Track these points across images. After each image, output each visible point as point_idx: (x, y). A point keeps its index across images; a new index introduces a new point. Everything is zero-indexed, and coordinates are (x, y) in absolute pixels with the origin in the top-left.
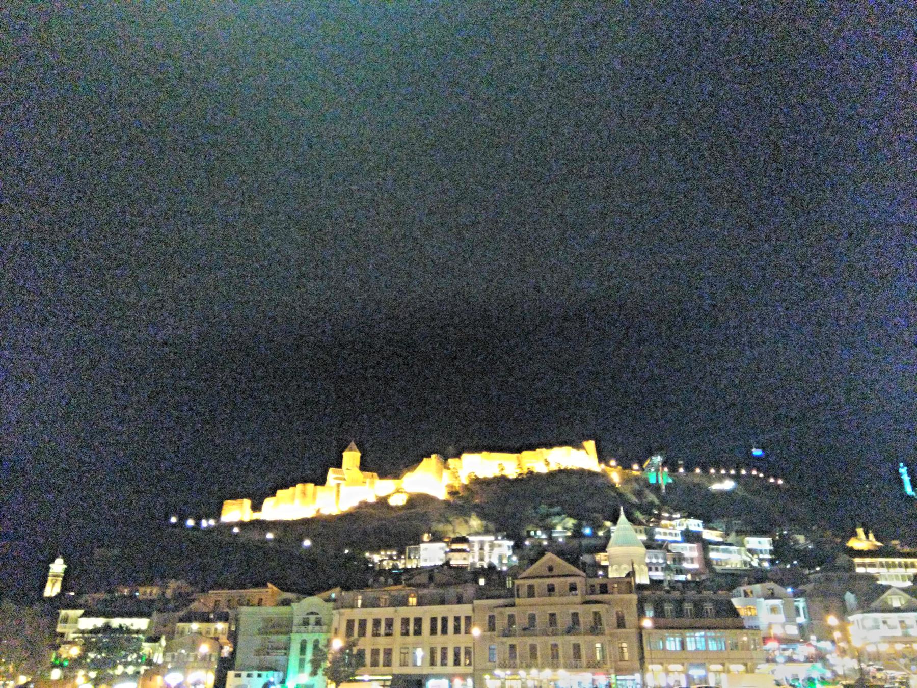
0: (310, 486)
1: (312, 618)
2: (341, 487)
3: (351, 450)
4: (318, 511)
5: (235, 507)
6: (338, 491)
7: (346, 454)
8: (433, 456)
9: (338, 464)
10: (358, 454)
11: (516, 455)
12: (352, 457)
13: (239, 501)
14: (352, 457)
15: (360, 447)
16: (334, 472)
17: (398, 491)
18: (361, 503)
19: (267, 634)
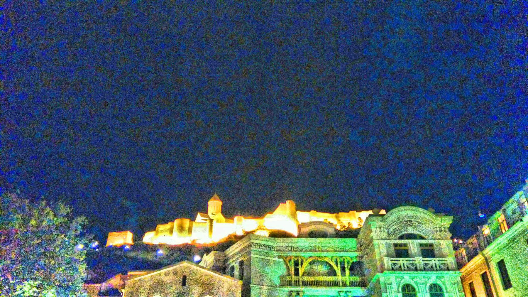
0: (187, 222)
1: (413, 246)
2: (214, 223)
3: (215, 199)
4: (194, 240)
5: (119, 237)
6: (211, 226)
7: (209, 203)
8: (288, 202)
9: (204, 210)
10: (220, 203)
11: (335, 214)
12: (214, 205)
13: (123, 233)
14: (214, 205)
15: (222, 197)
16: (202, 216)
17: (261, 229)
18: (230, 237)
19: (297, 283)
